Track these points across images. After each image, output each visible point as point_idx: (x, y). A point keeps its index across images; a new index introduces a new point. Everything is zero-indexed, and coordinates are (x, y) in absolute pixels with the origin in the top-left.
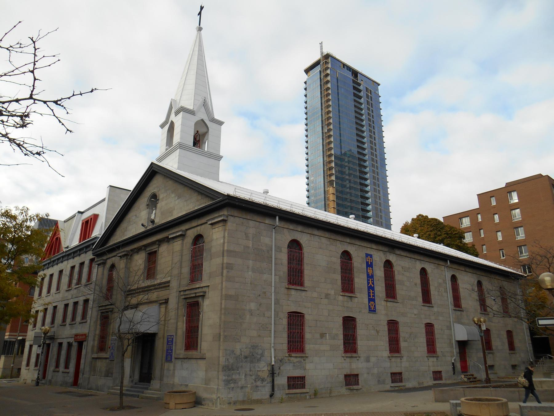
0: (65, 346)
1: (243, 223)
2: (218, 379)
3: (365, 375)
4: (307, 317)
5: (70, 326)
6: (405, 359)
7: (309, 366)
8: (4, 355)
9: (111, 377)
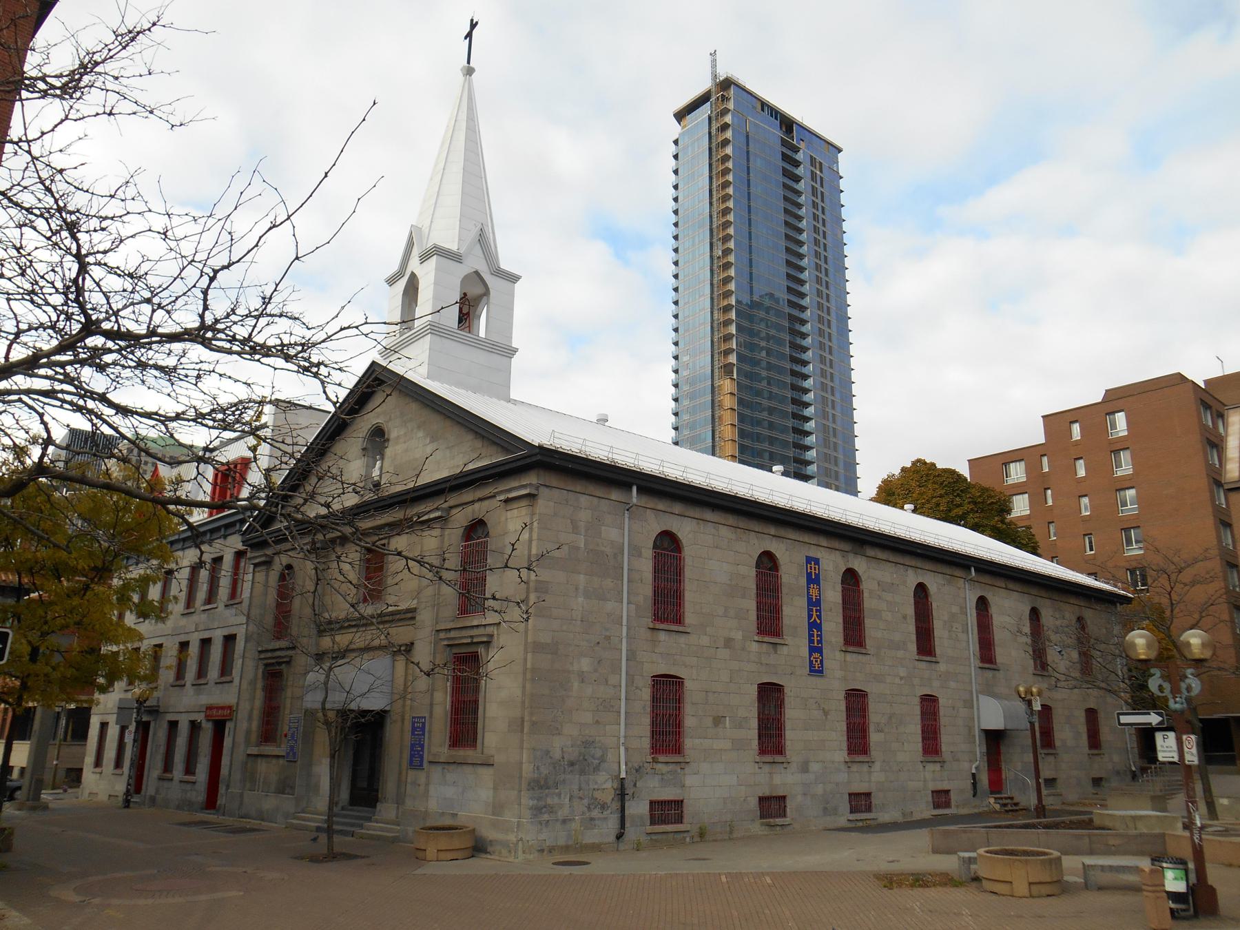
0: (184, 729)
1: (567, 501)
2: (520, 804)
3: (799, 798)
4: (688, 685)
5: (195, 687)
6: (877, 766)
7: (690, 780)
8: (29, 740)
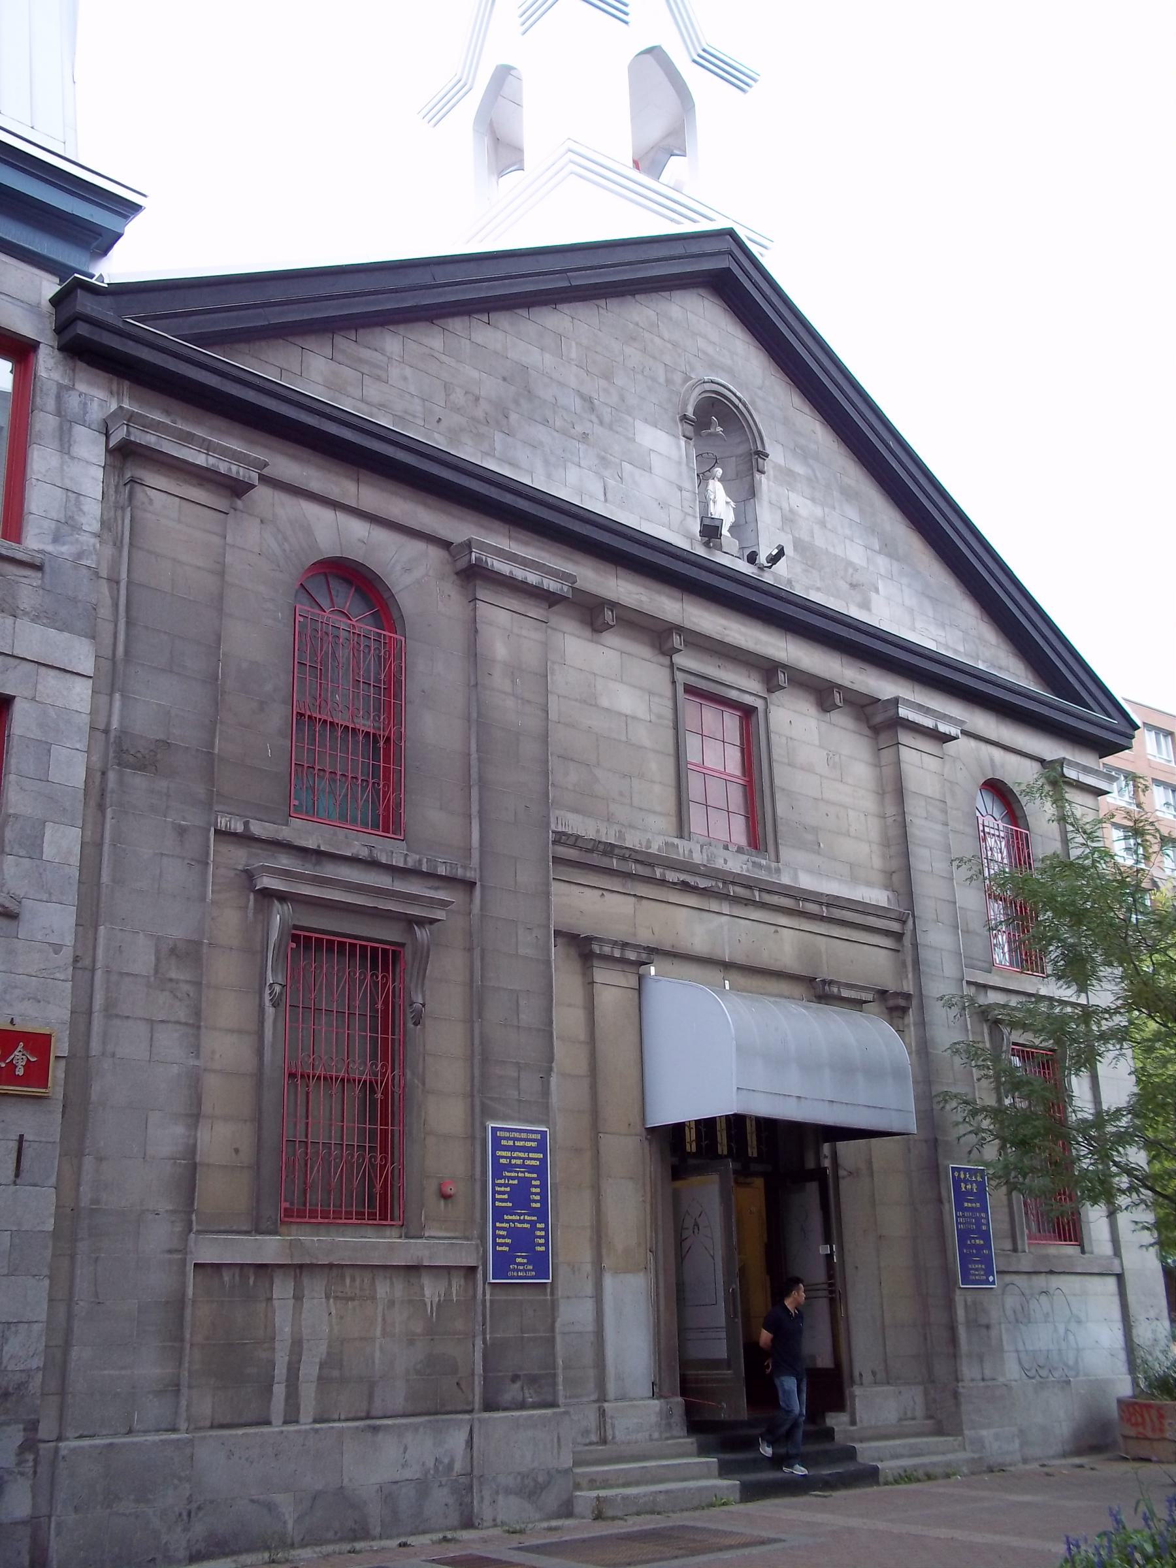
9: (535, 1406)
